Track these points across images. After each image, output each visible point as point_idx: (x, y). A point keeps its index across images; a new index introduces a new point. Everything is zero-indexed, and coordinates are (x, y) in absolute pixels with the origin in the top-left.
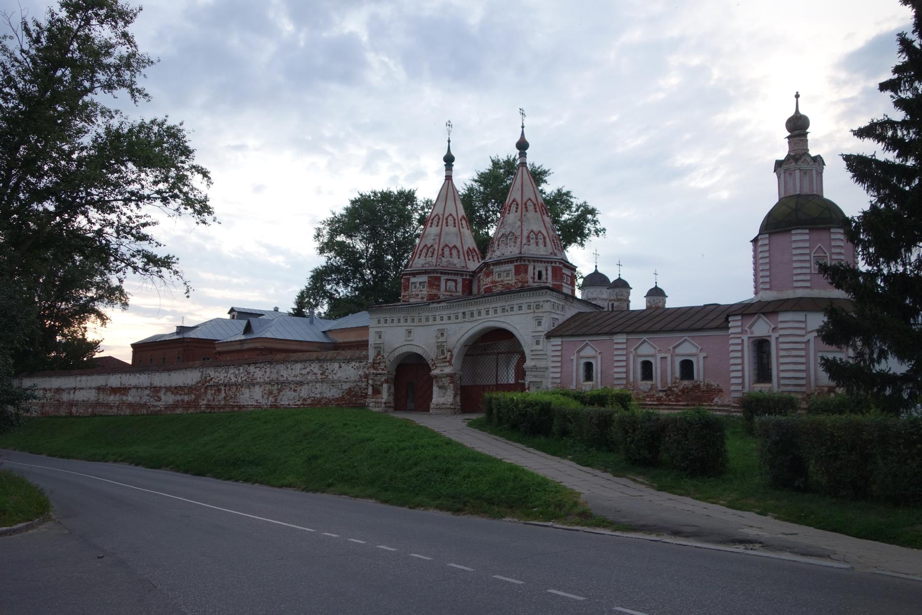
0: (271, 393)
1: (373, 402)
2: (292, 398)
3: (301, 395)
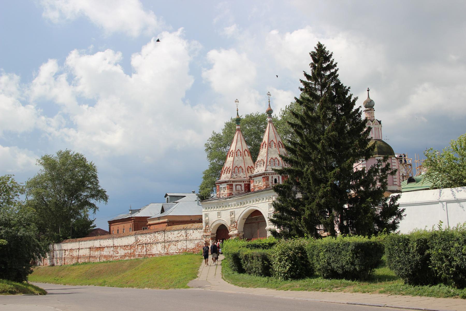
0: (165, 247)
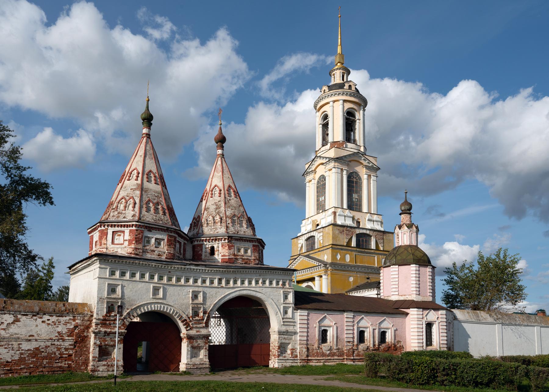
1: (104, 365)
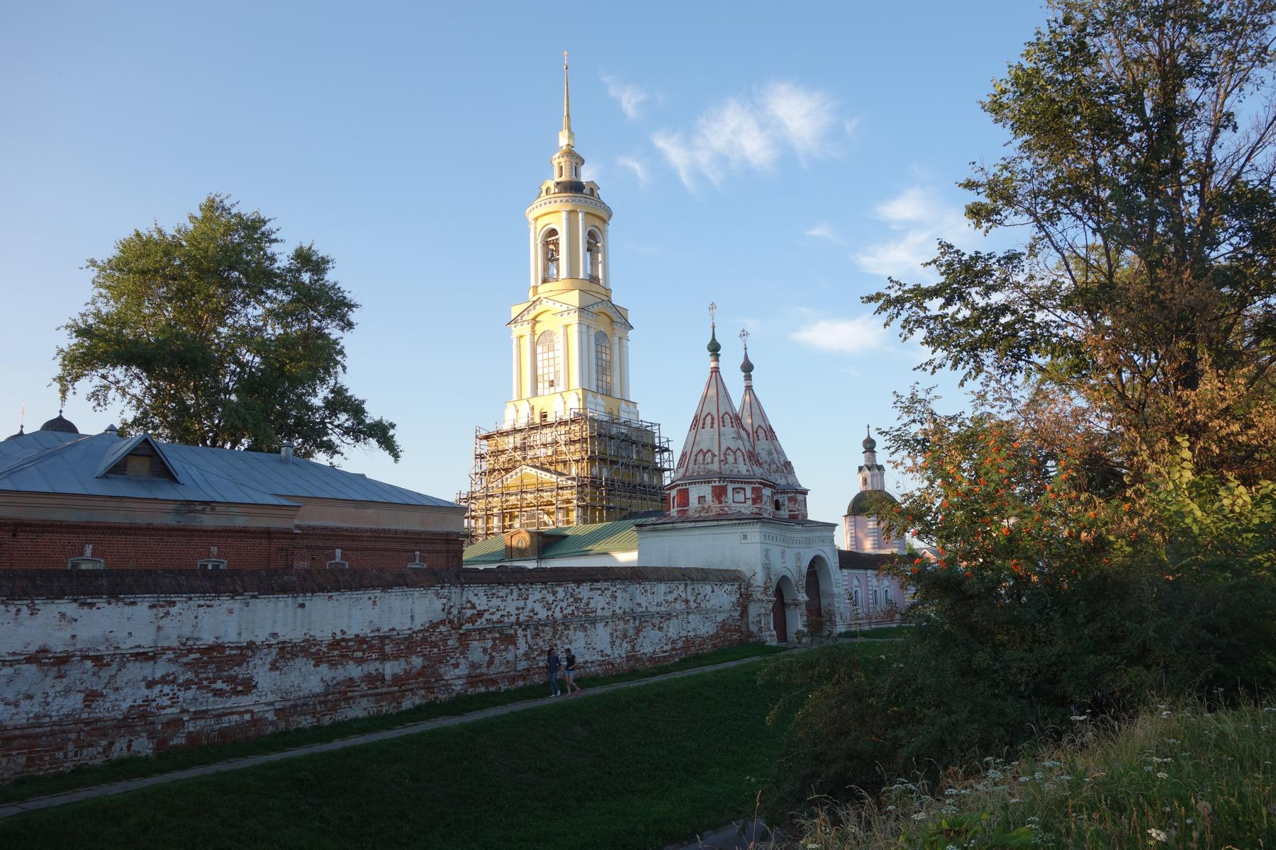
2: (657, 640)
3: (670, 634)
